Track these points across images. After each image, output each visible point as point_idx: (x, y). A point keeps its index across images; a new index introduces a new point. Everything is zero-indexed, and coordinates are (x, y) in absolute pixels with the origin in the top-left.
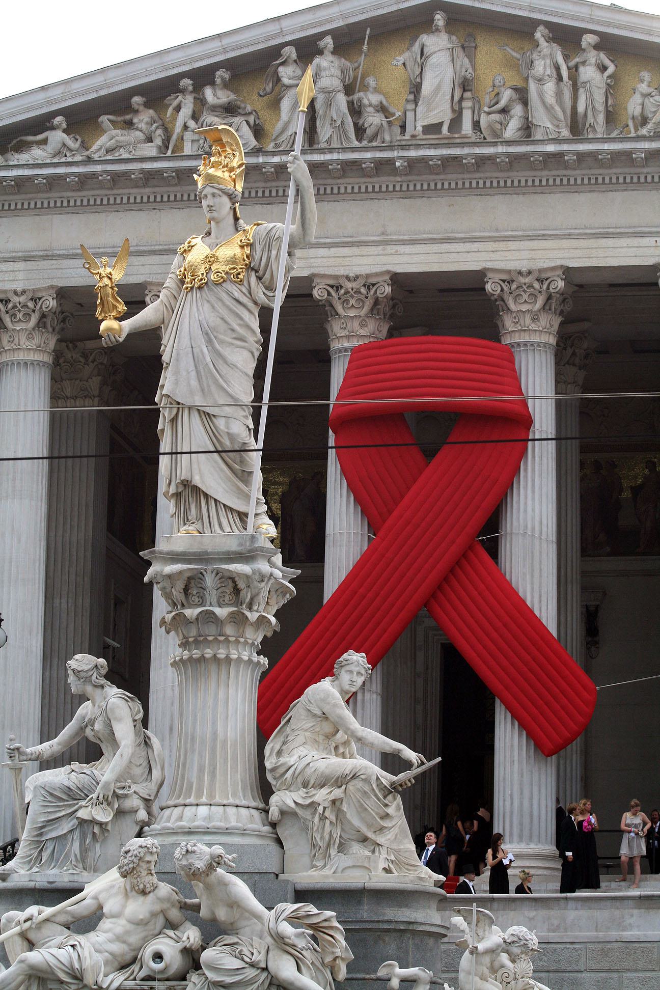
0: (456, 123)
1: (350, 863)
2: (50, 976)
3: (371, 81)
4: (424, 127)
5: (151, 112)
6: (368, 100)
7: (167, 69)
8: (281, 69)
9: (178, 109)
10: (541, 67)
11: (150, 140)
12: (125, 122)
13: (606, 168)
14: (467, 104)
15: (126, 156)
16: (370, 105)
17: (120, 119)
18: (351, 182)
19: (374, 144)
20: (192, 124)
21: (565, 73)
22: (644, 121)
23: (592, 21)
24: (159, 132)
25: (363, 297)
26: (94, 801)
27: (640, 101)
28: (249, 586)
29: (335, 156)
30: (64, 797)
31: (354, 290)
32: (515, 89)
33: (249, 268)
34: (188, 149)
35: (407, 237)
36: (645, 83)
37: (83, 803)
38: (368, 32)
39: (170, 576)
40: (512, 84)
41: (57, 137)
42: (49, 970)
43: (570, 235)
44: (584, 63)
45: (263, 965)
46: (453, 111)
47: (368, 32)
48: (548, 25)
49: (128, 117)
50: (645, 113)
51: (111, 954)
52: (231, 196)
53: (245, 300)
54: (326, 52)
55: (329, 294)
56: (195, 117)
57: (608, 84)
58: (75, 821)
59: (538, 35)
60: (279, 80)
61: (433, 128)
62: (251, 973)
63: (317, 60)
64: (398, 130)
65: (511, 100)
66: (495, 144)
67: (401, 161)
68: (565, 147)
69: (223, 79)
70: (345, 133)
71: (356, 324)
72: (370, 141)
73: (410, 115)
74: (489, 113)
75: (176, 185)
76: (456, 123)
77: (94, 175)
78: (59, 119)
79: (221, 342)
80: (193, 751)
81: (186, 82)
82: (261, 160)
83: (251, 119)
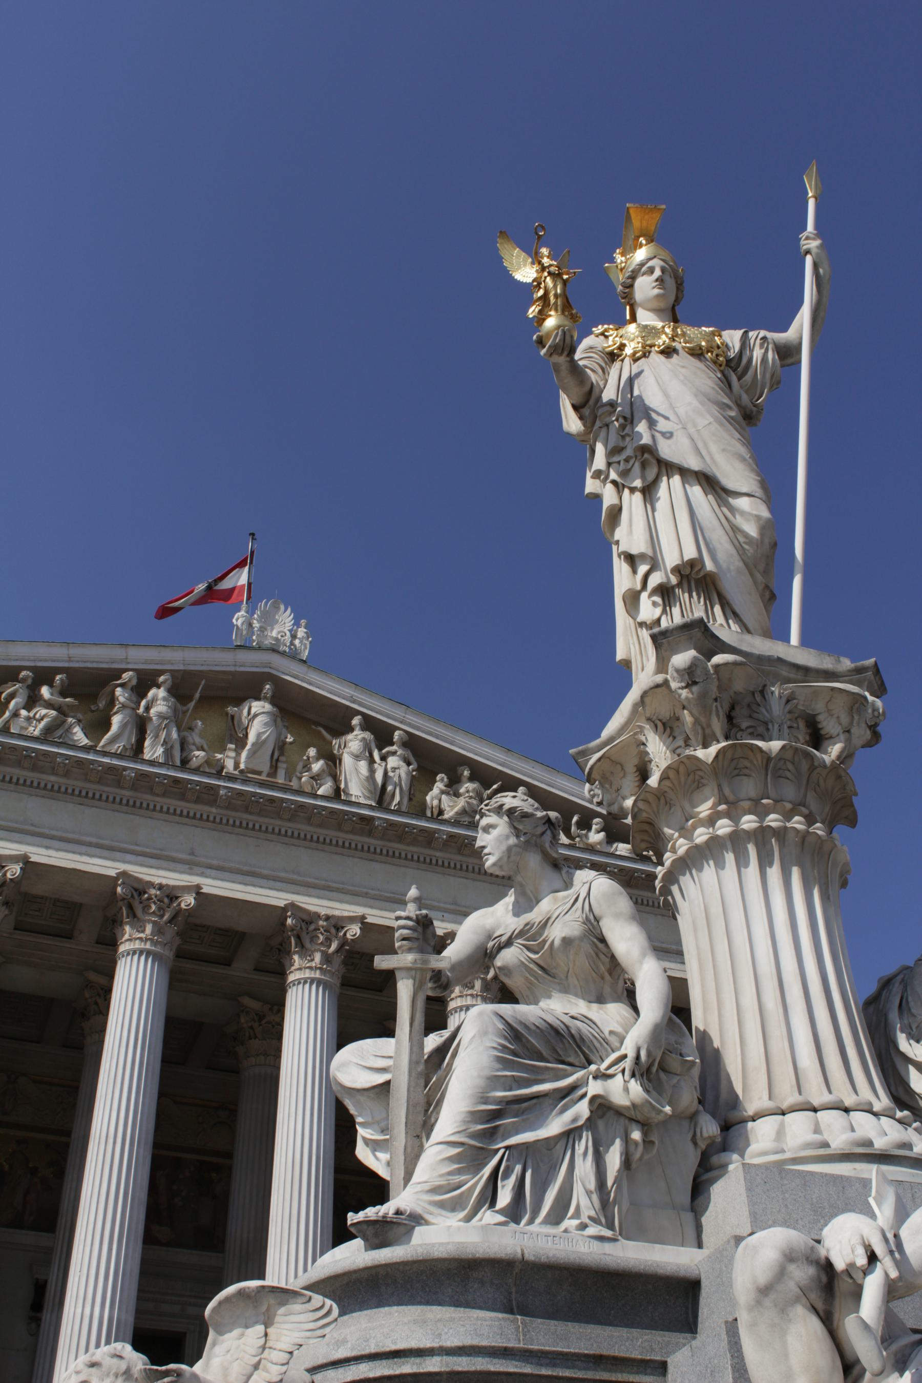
6: (193, 739)
7: (10, 660)
8: (119, 691)
9: (12, 696)
13: (408, 844)
16: (194, 744)
20: (24, 713)
25: (165, 906)
26: (628, 1064)
28: (848, 731)
30: (545, 1052)
31: (158, 898)
32: (327, 764)
35: (215, 862)
38: (203, 682)
43: (367, 893)
44: (394, 753)
46: (271, 766)
47: (203, 682)
48: (364, 716)
50: (442, 806)
55: (132, 896)
57: (413, 776)
58: (582, 1109)
59: (356, 721)
60: (112, 701)
65: (323, 771)
66: (315, 796)
67: (225, 791)
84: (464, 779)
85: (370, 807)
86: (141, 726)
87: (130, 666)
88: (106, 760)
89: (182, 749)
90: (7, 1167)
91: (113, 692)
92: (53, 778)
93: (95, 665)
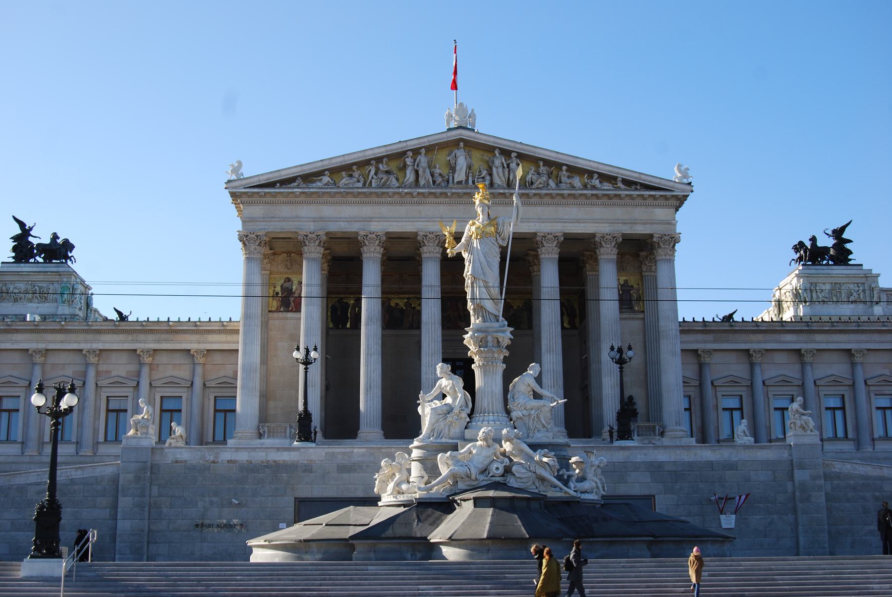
0: (467, 180)
1: (542, 435)
2: (458, 476)
3: (438, 166)
4: (457, 182)
5: (359, 172)
9: (370, 171)
10: (497, 162)
11: (359, 181)
12: (349, 174)
14: (470, 175)
15: (351, 186)
16: (437, 173)
17: (348, 173)
18: (431, 199)
19: (440, 187)
20: (375, 177)
21: (505, 166)
22: (532, 183)
23: (515, 148)
24: (362, 179)
27: (530, 176)
28: (503, 341)
29: (427, 191)
32: (487, 170)
33: (496, 232)
34: (373, 185)
36: (532, 170)
37: (448, 416)
38: (437, 147)
39: (477, 337)
40: (485, 168)
41: (326, 179)
42: (459, 474)
44: (512, 162)
45: (534, 471)
46: (466, 177)
47: (437, 147)
48: (500, 149)
49: (351, 173)
51: (479, 468)
52: (489, 208)
53: (494, 243)
54: (423, 154)
56: (376, 174)
61: (460, 183)
62: (530, 474)
63: (419, 157)
64: (446, 183)
65: (486, 174)
68: (506, 191)
69: (386, 161)
70: (429, 182)
71: (432, 248)
72: (437, 186)
73: (451, 178)
74: (478, 178)
75: (369, 198)
76: (467, 180)
77: (340, 193)
78: (326, 172)
79: (489, 257)
80: (485, 397)
81: (373, 162)
82: (401, 190)
83: (395, 176)
84: (541, 167)
85: (503, 188)
86: (417, 172)
87: (409, 148)
88: (406, 191)
89: (432, 178)
90: (404, 308)
91: (405, 159)
92: (389, 199)
93: (396, 151)
